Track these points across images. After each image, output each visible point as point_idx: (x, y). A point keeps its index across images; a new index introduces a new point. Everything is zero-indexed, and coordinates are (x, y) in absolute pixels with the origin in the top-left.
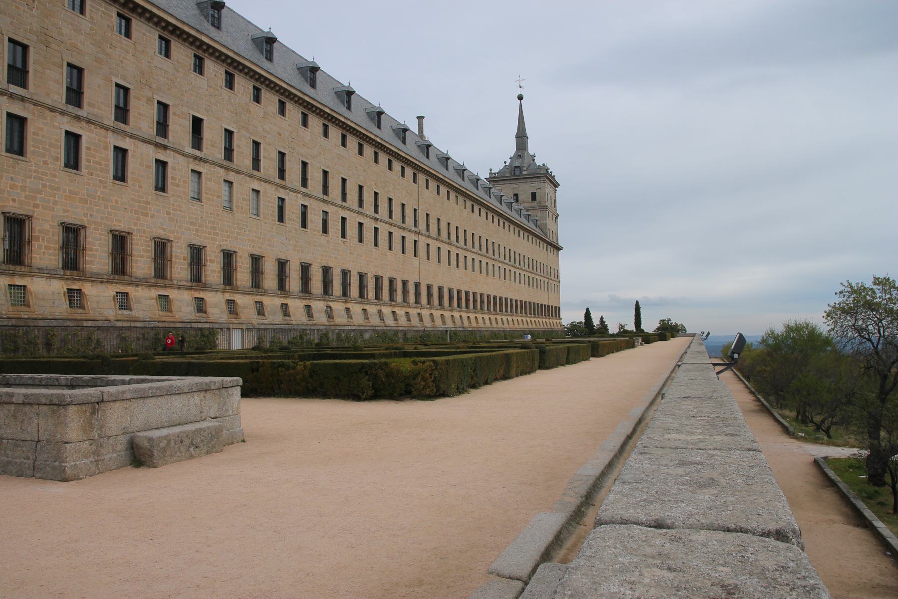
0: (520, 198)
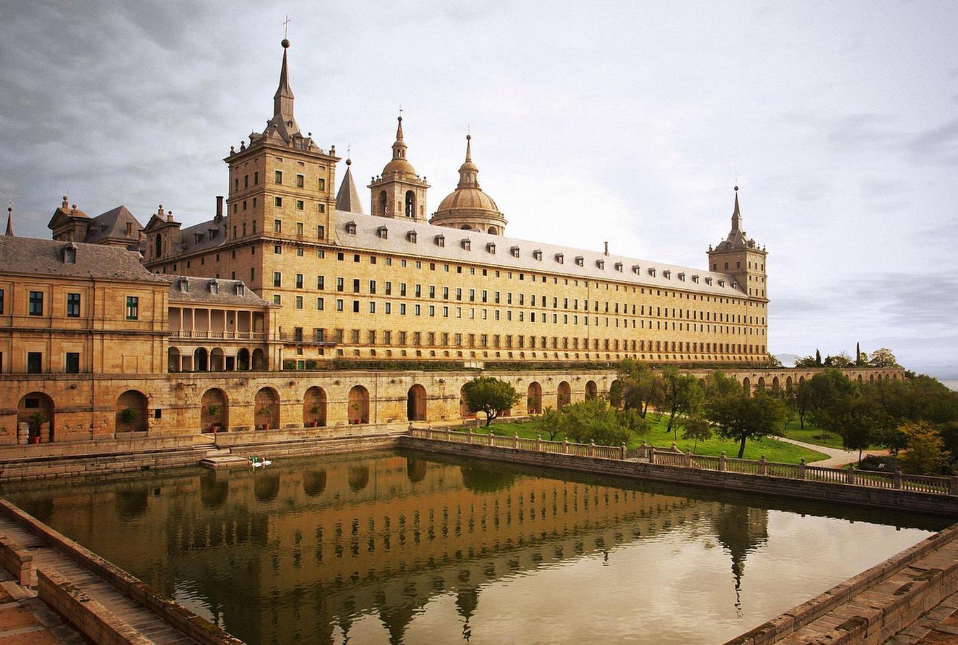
0: (729, 266)
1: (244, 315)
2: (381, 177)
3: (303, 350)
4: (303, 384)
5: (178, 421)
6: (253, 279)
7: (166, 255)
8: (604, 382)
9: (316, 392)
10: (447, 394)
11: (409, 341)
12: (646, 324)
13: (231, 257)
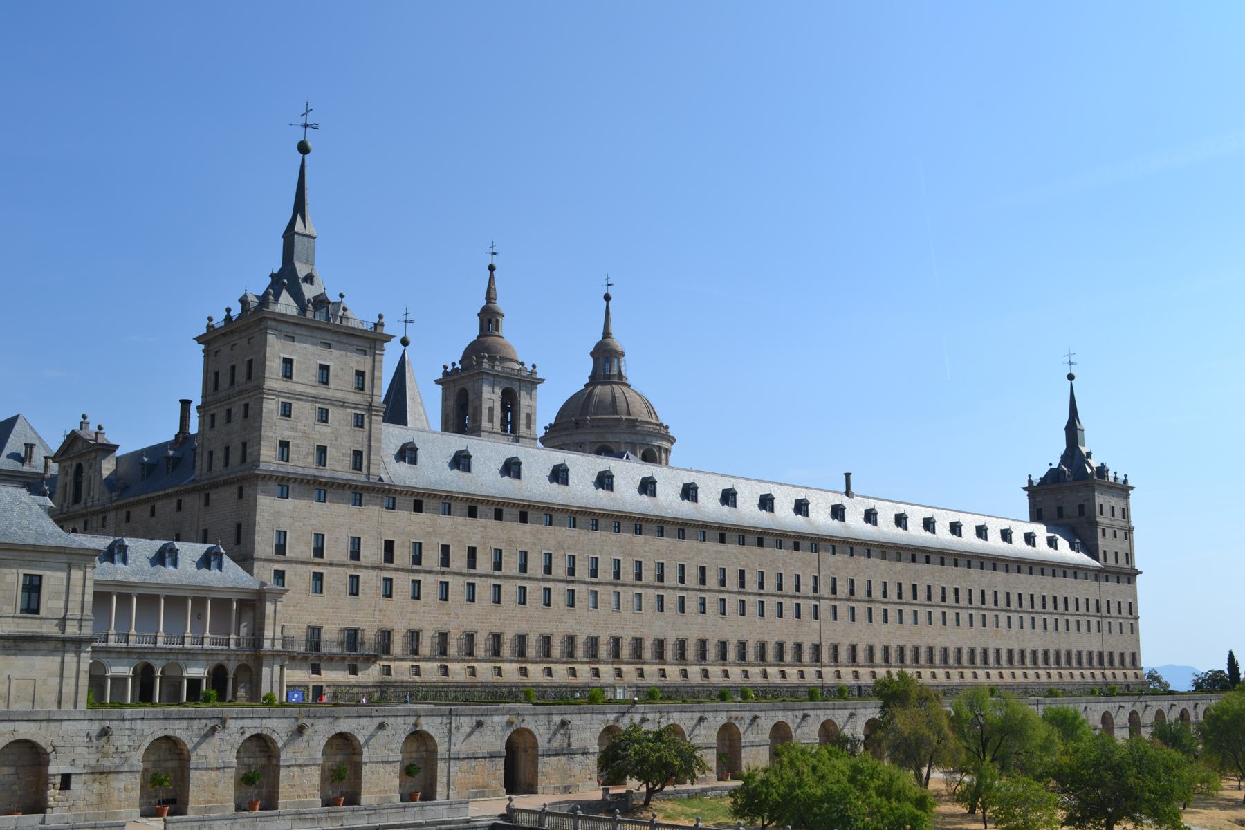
1: (221, 605)
2: (458, 366)
3: (322, 665)
4: (321, 732)
5: (100, 795)
6: (238, 542)
7: (90, 500)
8: (854, 722)
9: (344, 744)
10: (574, 746)
11: (506, 651)
12: (922, 616)
13: (202, 502)
